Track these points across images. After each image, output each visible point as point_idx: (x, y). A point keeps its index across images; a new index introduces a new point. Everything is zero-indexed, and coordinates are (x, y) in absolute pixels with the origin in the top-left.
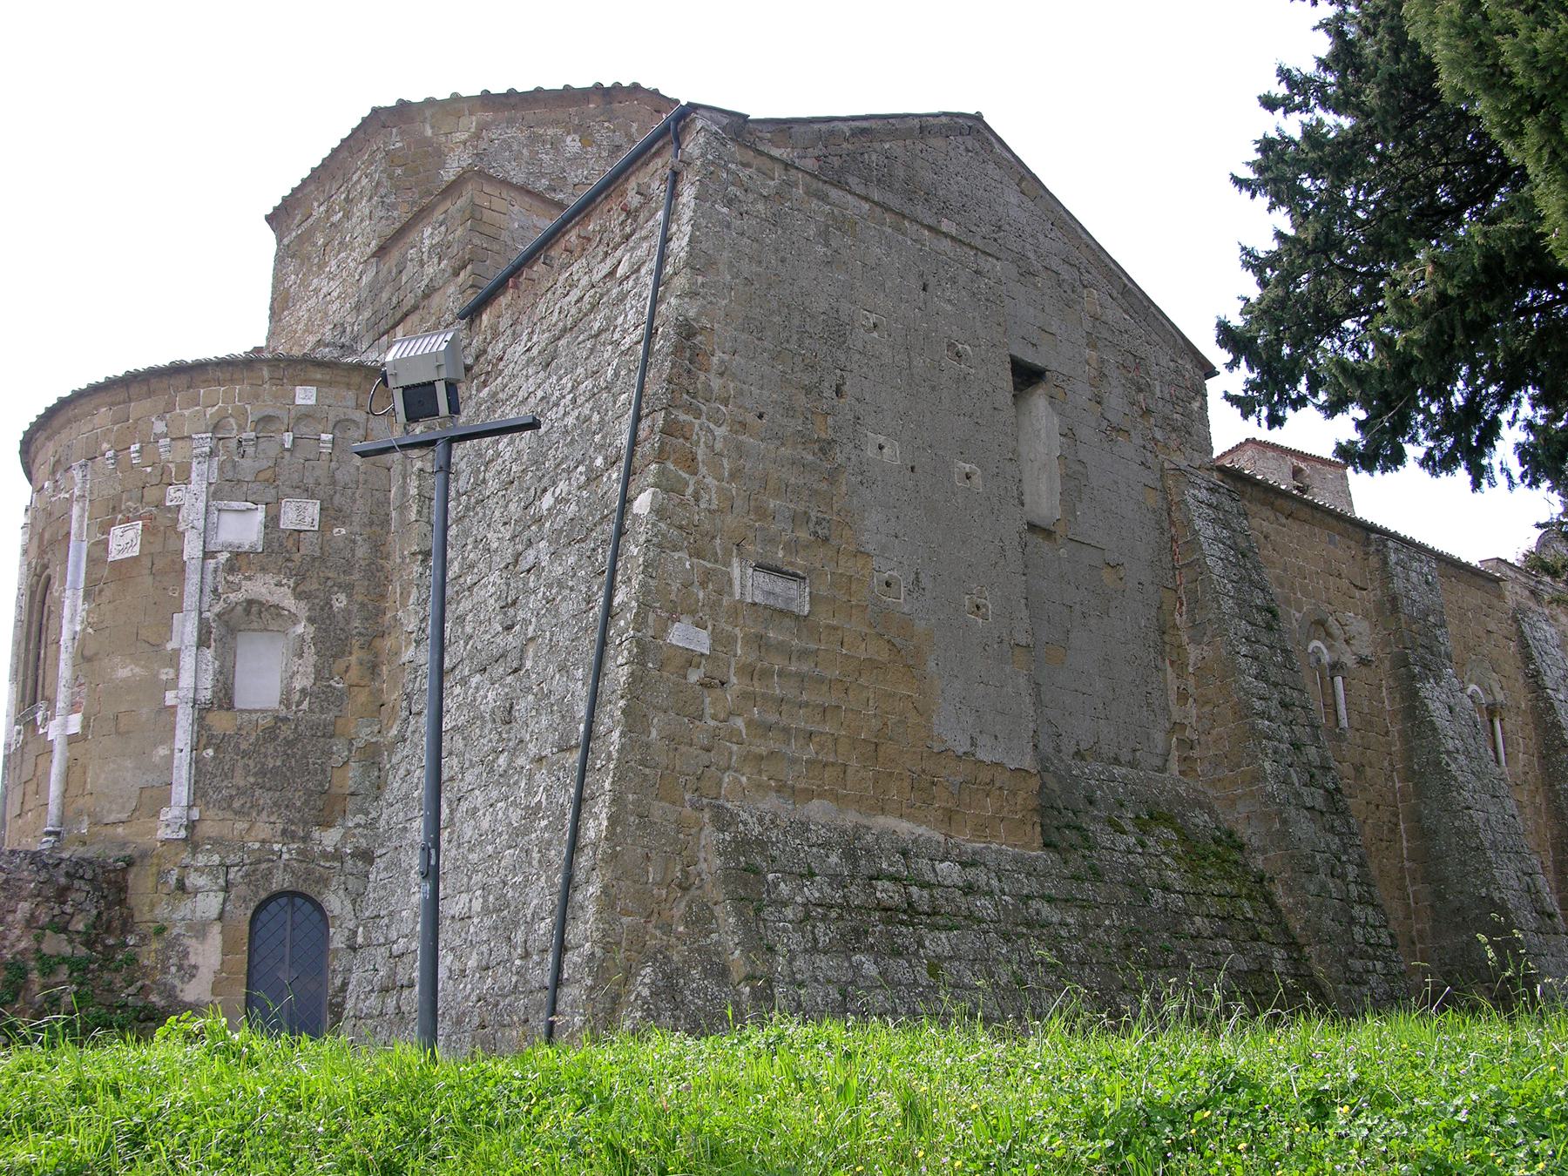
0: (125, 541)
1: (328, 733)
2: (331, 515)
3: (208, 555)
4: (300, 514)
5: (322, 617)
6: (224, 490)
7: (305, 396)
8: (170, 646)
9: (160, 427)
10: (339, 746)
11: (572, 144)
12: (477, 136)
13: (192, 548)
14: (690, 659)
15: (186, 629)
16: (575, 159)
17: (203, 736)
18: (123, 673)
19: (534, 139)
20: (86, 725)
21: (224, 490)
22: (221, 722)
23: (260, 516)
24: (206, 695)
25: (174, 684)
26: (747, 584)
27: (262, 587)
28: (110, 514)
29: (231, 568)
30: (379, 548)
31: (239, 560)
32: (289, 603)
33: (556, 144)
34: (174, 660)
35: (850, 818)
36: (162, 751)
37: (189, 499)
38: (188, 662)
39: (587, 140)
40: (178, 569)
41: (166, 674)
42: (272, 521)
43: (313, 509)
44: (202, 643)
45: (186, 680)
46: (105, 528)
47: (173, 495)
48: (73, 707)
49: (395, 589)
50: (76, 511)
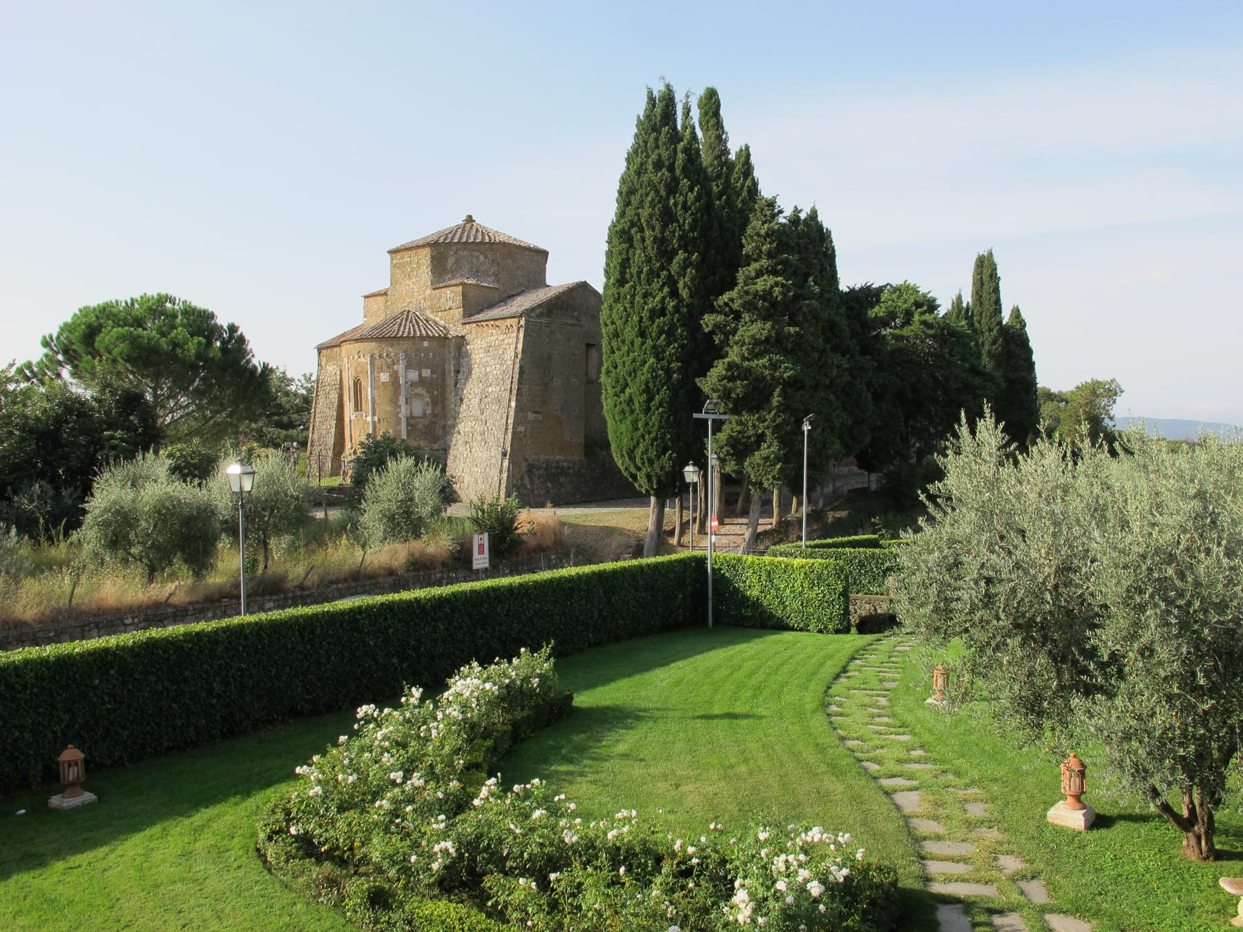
1: (435, 423)
2: (432, 372)
4: (426, 373)
5: (432, 397)
7: (426, 344)
11: (482, 258)
12: (456, 253)
13: (402, 381)
14: (521, 432)
17: (408, 424)
19: (471, 255)
22: (412, 421)
23: (417, 373)
26: (531, 416)
27: (419, 390)
29: (411, 385)
30: (444, 380)
31: (413, 384)
32: (425, 394)
33: (478, 257)
35: (547, 457)
39: (486, 257)
42: (420, 375)
49: (448, 390)
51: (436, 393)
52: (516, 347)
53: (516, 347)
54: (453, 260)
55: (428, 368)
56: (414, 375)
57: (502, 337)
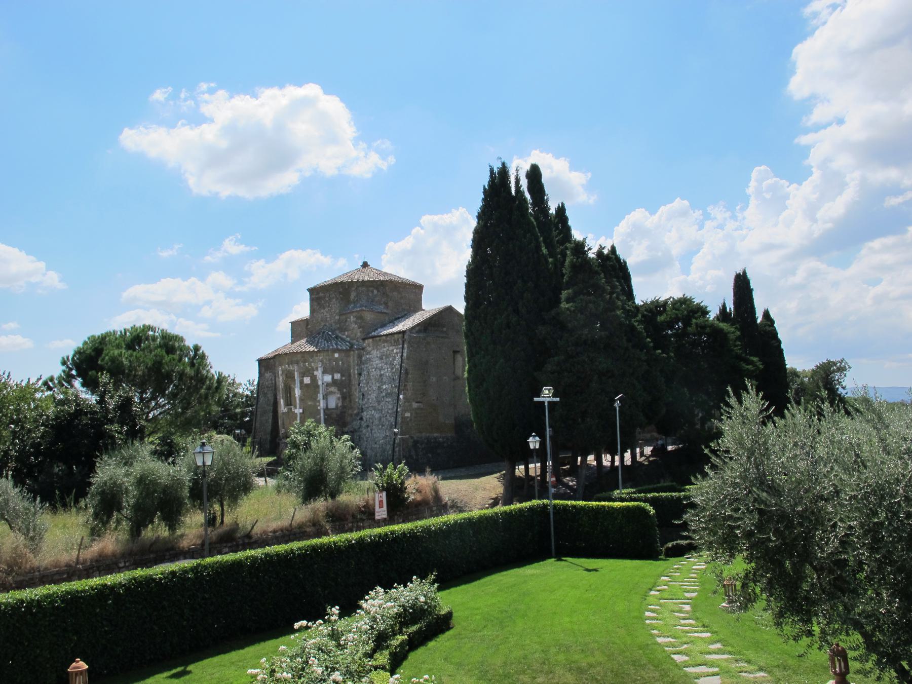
0: (307, 380)
1: (345, 412)
2: (342, 376)
3: (323, 384)
4: (337, 376)
5: (342, 393)
6: (324, 372)
7: (336, 355)
8: (318, 399)
9: (311, 360)
10: (346, 415)
11: (375, 292)
12: (356, 289)
13: (320, 383)
14: (408, 417)
15: (320, 396)
16: (376, 296)
17: (325, 414)
18: (310, 403)
20: (303, 411)
21: (324, 372)
22: (328, 412)
24: (325, 407)
25: (319, 406)
26: (415, 405)
27: (333, 389)
28: (303, 375)
30: (350, 381)
31: (328, 385)
33: (372, 292)
34: (319, 401)
35: (428, 435)
36: (318, 417)
37: (318, 373)
38: (322, 402)
39: (378, 291)
40: (318, 386)
41: (318, 404)
42: (333, 378)
43: (339, 375)
44: (323, 399)
45: (322, 405)
46: (303, 377)
47: (315, 373)
48: (300, 408)
49: (353, 388)
50: (296, 373)
51: (345, 390)
52: (402, 356)
53: (402, 356)
54: (355, 294)
55: (339, 373)
56: (328, 378)
57: (391, 348)
